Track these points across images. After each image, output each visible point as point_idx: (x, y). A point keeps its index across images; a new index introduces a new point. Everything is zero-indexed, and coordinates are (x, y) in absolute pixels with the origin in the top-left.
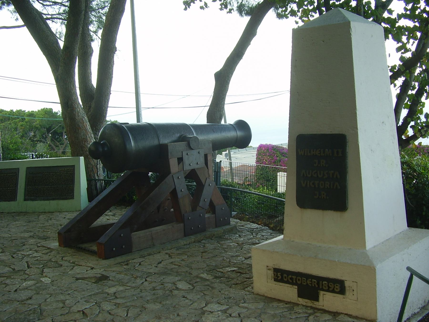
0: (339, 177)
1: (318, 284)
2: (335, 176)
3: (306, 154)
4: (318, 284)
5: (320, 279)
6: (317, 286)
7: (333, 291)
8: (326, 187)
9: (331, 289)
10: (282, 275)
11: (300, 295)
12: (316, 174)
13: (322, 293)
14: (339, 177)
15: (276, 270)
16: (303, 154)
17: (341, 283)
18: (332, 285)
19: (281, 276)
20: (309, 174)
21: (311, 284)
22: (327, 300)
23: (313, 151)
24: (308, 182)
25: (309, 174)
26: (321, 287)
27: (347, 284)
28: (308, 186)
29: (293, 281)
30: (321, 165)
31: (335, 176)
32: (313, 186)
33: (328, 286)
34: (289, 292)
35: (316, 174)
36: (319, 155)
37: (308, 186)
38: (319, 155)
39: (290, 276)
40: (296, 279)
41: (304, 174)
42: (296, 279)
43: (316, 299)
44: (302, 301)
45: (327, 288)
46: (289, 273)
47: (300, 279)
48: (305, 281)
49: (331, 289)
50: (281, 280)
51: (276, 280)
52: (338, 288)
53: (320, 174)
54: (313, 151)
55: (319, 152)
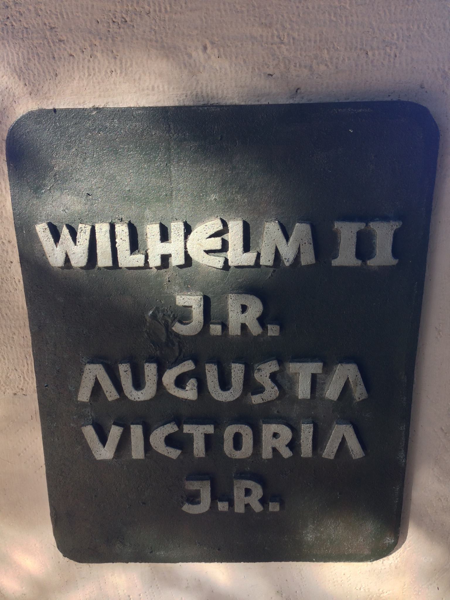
2: (332, 392)
3: (104, 259)
8: (267, 453)
12: (192, 384)
14: (359, 392)
16: (79, 259)
20: (138, 384)
23: (165, 236)
24: (137, 431)
25: (138, 384)
30: (234, 330)
32: (174, 453)
35: (192, 384)
37: (137, 451)
38: (217, 262)
41: (97, 388)
53: (225, 383)
54: (165, 236)
55: (216, 244)
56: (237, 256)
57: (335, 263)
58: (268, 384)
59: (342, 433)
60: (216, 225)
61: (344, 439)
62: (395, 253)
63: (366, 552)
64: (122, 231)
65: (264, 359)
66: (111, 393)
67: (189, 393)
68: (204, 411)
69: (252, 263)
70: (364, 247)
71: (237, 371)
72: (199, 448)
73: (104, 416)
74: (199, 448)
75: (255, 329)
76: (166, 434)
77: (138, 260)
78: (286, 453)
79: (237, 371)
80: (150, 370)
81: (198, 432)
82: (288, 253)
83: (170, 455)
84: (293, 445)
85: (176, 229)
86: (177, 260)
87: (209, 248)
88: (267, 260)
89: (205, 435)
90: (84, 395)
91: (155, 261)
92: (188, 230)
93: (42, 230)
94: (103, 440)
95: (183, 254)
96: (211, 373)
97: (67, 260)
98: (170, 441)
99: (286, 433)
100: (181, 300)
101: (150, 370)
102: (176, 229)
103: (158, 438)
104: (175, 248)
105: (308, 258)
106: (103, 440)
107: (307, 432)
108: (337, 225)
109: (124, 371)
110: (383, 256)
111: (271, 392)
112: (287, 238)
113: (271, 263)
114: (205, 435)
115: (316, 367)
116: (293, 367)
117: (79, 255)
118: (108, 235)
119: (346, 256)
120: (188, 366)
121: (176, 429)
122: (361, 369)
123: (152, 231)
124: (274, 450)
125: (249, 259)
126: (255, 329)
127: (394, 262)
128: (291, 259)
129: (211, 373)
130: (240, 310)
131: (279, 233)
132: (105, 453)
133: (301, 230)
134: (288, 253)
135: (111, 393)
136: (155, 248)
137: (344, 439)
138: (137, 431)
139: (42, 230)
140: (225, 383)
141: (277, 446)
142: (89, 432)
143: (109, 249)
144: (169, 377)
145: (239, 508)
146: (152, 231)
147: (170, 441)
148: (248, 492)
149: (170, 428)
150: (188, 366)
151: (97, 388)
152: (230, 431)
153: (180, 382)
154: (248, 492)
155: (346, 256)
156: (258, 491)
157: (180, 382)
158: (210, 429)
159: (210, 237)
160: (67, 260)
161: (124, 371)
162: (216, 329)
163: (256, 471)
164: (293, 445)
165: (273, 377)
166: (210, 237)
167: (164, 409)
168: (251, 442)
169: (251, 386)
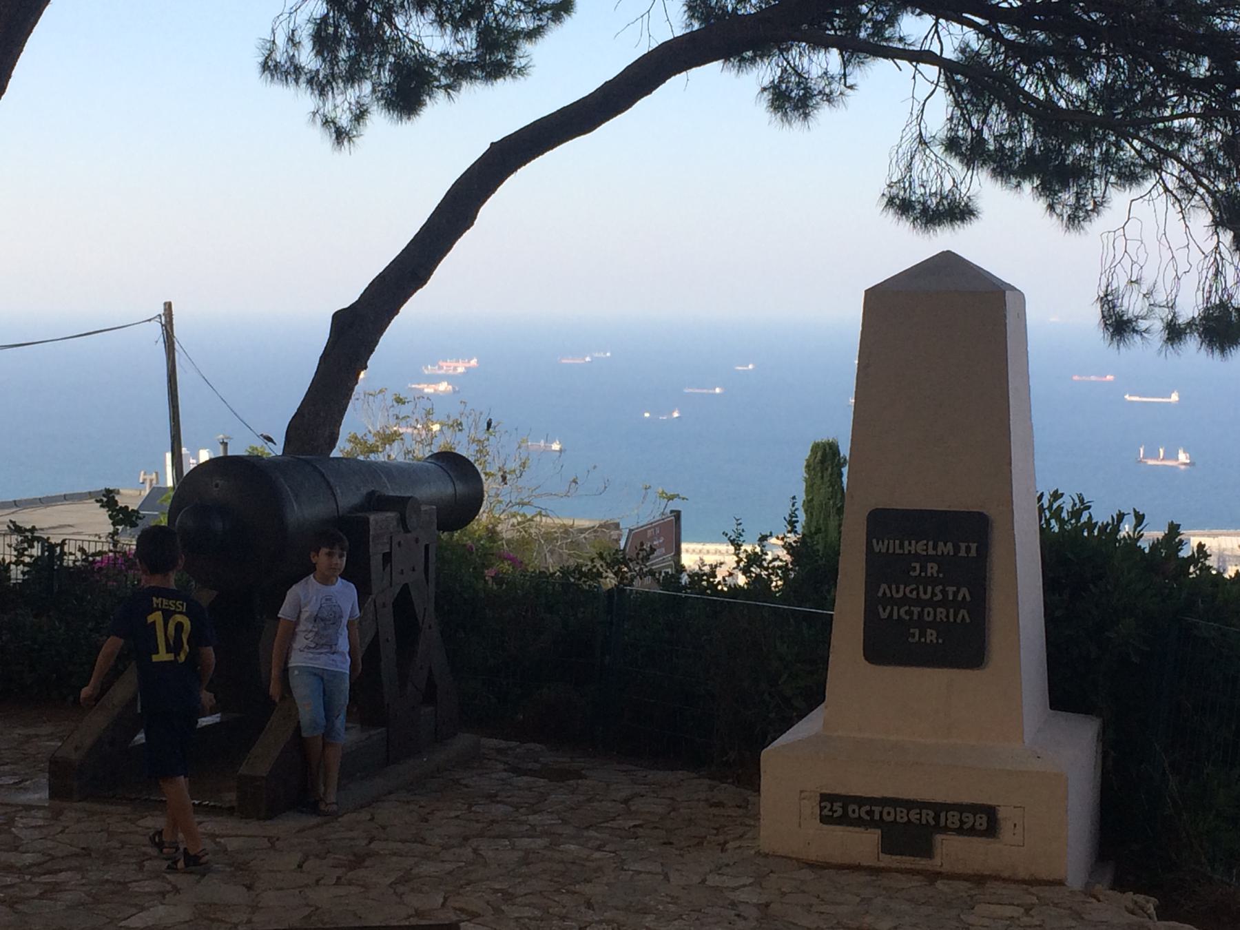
0: (968, 598)
1: (937, 818)
2: (960, 598)
3: (891, 551)
4: (937, 818)
5: (939, 808)
6: (933, 823)
7: (972, 832)
9: (966, 827)
10: (845, 808)
11: (888, 846)
13: (939, 837)
14: (968, 598)
15: (827, 798)
16: (884, 551)
17: (990, 812)
18: (969, 819)
19: (839, 809)
20: (898, 592)
21: (920, 820)
22: (953, 851)
23: (910, 544)
24: (896, 608)
25: (898, 592)
26: (942, 823)
27: (1002, 813)
28: (895, 617)
29: (872, 819)
31: (960, 598)
33: (961, 820)
34: (862, 844)
37: (895, 617)
39: (868, 808)
40: (881, 813)
41: (884, 593)
42: (881, 813)
43: (928, 853)
44: (887, 860)
45: (958, 824)
46: (861, 801)
47: (892, 811)
48: (904, 815)
49: (966, 827)
50: (844, 820)
51: (825, 820)
52: (982, 822)
53: (925, 593)
54: (910, 544)
56: (931, 552)
59: (963, 612)
64: (897, 542)
68: (918, 602)
70: (968, 549)
71: (929, 589)
72: (915, 617)
74: (915, 617)
79: (929, 589)
80: (902, 587)
81: (916, 610)
84: (947, 616)
90: (880, 594)
93: (874, 541)
98: (906, 612)
101: (902, 587)
103: (902, 611)
107: (952, 611)
110: (973, 553)
111: (940, 597)
123: (906, 543)
129: (921, 588)
133: (950, 545)
138: (896, 608)
139: (874, 541)
140: (925, 593)
144: (908, 590)
146: (906, 543)
151: (884, 593)
152: (926, 610)
153: (911, 592)
155: (963, 553)
157: (911, 592)
161: (894, 587)
163: (932, 625)
164: (947, 616)
167: (905, 600)
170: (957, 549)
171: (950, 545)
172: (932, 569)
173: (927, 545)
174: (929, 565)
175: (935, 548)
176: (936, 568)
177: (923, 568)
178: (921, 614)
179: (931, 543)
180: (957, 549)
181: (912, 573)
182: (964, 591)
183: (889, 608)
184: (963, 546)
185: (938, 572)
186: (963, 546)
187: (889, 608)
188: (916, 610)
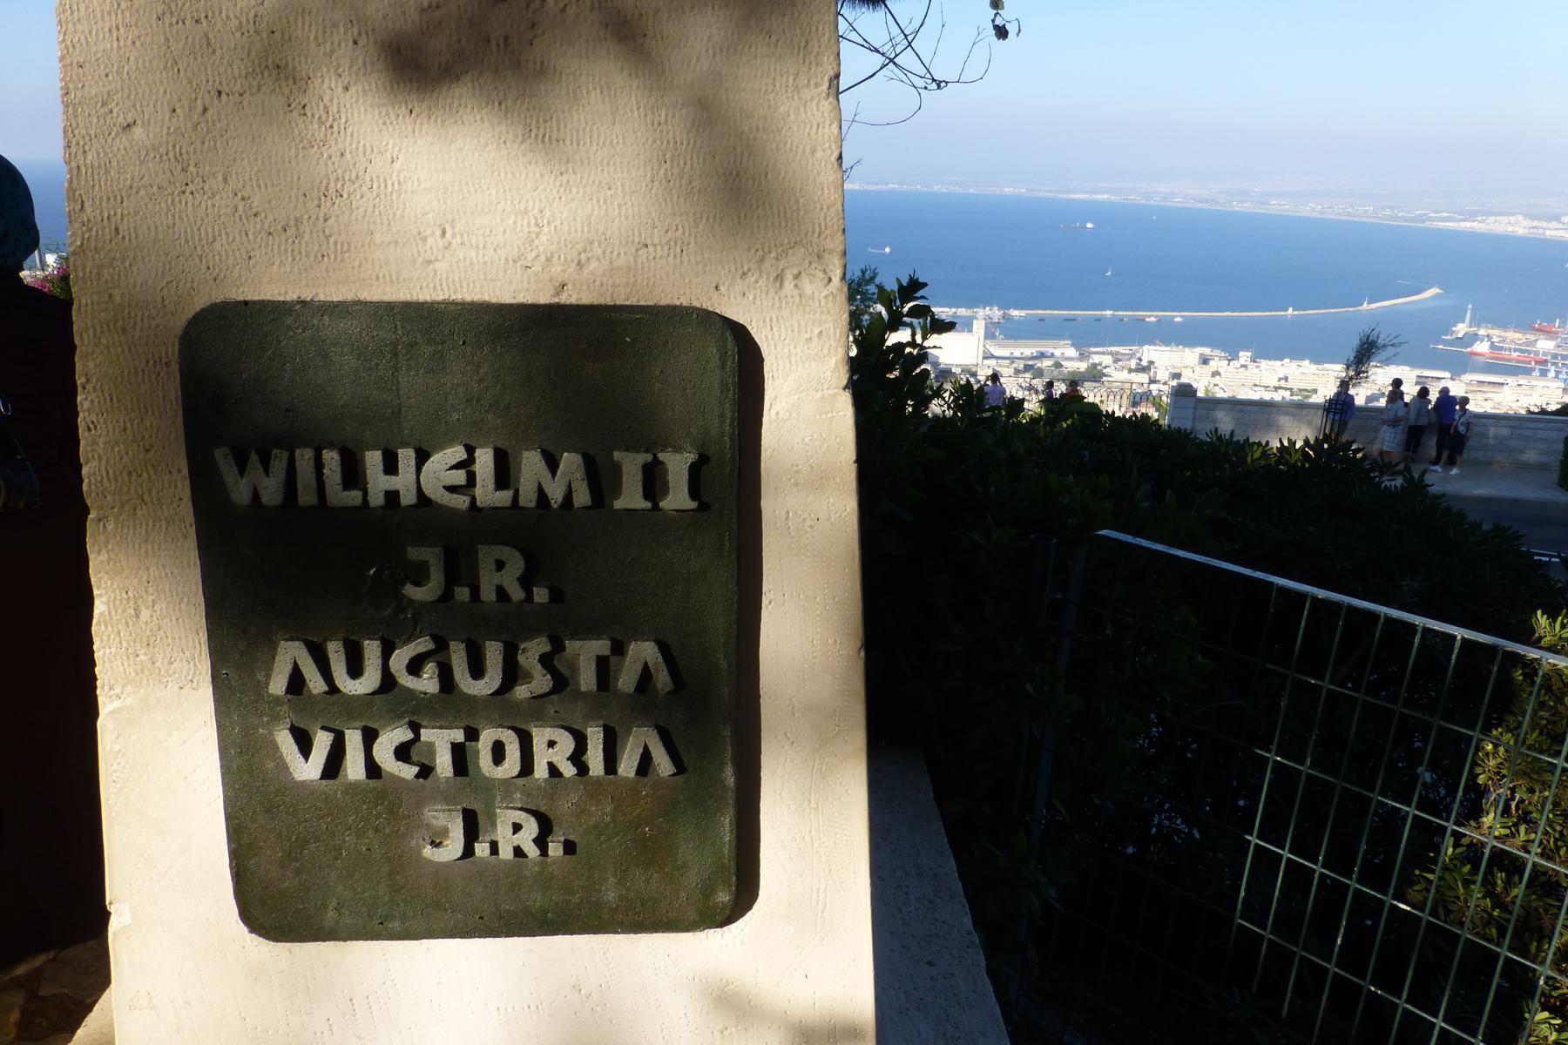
2: (626, 681)
3: (306, 497)
12: (430, 669)
14: (663, 679)
20: (355, 671)
23: (391, 467)
24: (354, 739)
25: (355, 671)
30: (488, 594)
32: (408, 772)
35: (430, 669)
36: (460, 502)
37: (354, 768)
53: (477, 671)
55: (460, 477)
56: (487, 493)
57: (619, 504)
58: (537, 670)
60: (457, 453)
61: (646, 748)
62: (694, 493)
63: (692, 915)
64: (331, 457)
65: (531, 633)
66: (316, 684)
67: (427, 682)
69: (508, 504)
71: (494, 653)
73: (307, 711)
74: (444, 763)
75: (517, 594)
76: (396, 743)
77: (354, 497)
78: (568, 770)
79: (494, 653)
81: (441, 741)
82: (556, 493)
83: (402, 775)
84: (578, 758)
85: (406, 457)
86: (408, 498)
87: (449, 483)
88: (528, 498)
89: (453, 744)
91: (376, 499)
92: (422, 457)
93: (222, 457)
94: (305, 747)
95: (414, 491)
96: (458, 657)
97: (256, 496)
98: (403, 753)
99: (567, 743)
100: (415, 553)
102: (406, 457)
103: (384, 751)
104: (403, 481)
105: (582, 498)
106: (305, 747)
108: (617, 455)
109: (336, 653)
110: (678, 498)
111: (541, 682)
112: (554, 474)
113: (533, 504)
114: (453, 744)
115: (601, 646)
116: (571, 646)
117: (271, 489)
118: (312, 463)
119: (631, 498)
120: (423, 644)
121: (410, 735)
122: (663, 647)
123: (374, 459)
124: (551, 766)
125: (503, 498)
126: (517, 594)
127: (693, 505)
128: (560, 500)
130: (493, 567)
131: (542, 465)
132: (309, 770)
133: (570, 461)
134: (556, 493)
135: (316, 684)
136: (378, 482)
137: (646, 748)
138: (354, 739)
139: (222, 457)
140: (477, 671)
141: (554, 760)
142: (286, 742)
143: (314, 483)
145: (506, 853)
146: (374, 459)
147: (403, 753)
148: (517, 828)
149: (402, 734)
150: (423, 644)
152: (487, 737)
153: (415, 667)
154: (517, 828)
155: (631, 498)
156: (531, 828)
157: (415, 667)
158: (459, 736)
159: (452, 468)
160: (256, 496)
161: (336, 653)
162: (463, 594)
165: (546, 661)
166: (452, 468)
168: (518, 754)
169: (512, 674)
170: (602, 479)
171: (570, 461)
172: (498, 573)
173: (467, 464)
174: (486, 555)
175: (504, 474)
176: (516, 564)
177: (459, 569)
178: (459, 752)
179: (484, 460)
180: (602, 479)
181: (414, 593)
182: (643, 651)
183: (322, 742)
184: (631, 464)
185: (526, 582)
186: (631, 464)
187: (322, 742)
188: (441, 741)
